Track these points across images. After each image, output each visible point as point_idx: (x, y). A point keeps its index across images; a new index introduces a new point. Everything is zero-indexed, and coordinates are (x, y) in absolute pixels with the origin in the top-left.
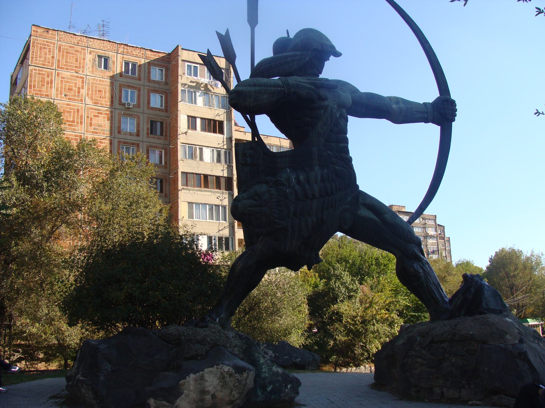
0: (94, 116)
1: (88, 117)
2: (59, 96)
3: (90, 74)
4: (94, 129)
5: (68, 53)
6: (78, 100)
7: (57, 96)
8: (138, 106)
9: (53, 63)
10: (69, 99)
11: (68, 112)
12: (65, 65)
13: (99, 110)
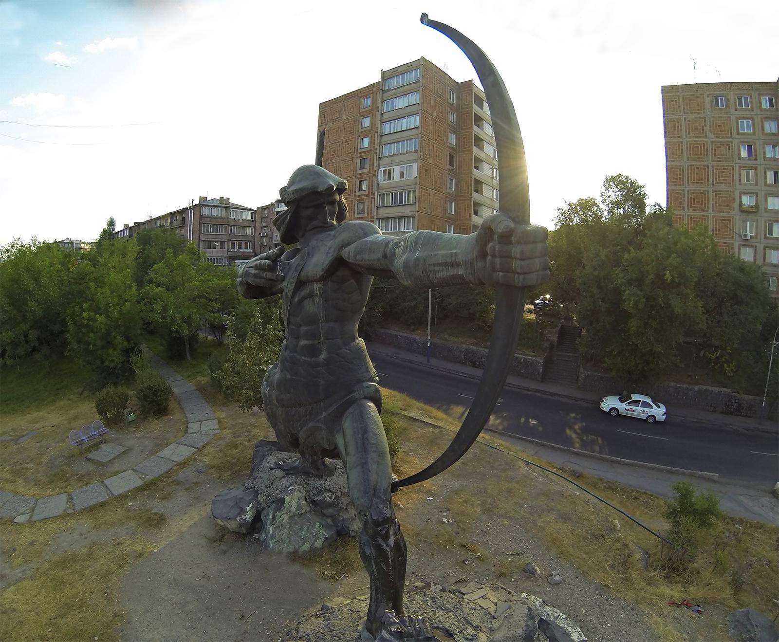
0: (718, 147)
1: (712, 149)
2: (688, 135)
3: (710, 114)
4: (719, 158)
5: (690, 100)
6: (703, 137)
7: (686, 136)
8: (754, 133)
9: (680, 111)
10: (696, 137)
11: (697, 147)
12: (689, 110)
13: (720, 142)
